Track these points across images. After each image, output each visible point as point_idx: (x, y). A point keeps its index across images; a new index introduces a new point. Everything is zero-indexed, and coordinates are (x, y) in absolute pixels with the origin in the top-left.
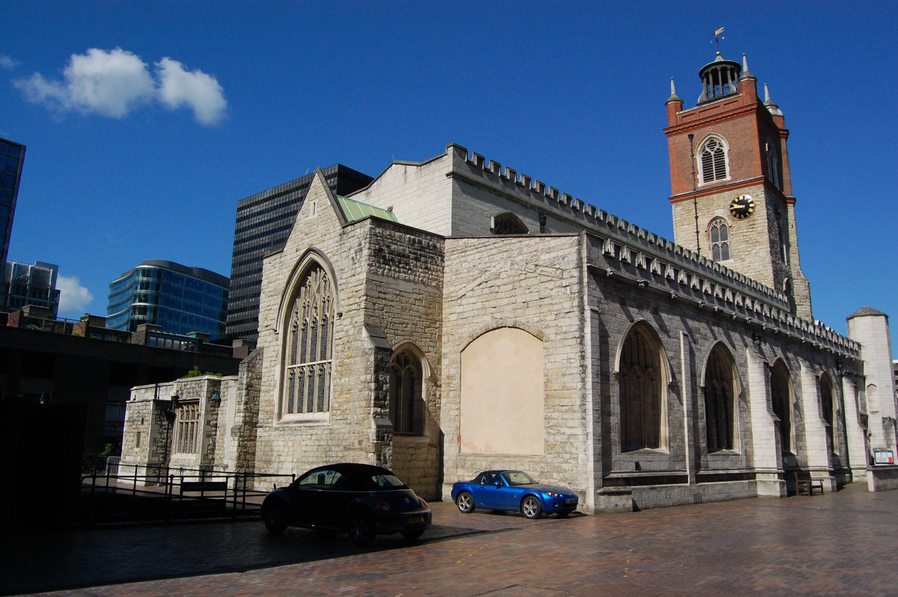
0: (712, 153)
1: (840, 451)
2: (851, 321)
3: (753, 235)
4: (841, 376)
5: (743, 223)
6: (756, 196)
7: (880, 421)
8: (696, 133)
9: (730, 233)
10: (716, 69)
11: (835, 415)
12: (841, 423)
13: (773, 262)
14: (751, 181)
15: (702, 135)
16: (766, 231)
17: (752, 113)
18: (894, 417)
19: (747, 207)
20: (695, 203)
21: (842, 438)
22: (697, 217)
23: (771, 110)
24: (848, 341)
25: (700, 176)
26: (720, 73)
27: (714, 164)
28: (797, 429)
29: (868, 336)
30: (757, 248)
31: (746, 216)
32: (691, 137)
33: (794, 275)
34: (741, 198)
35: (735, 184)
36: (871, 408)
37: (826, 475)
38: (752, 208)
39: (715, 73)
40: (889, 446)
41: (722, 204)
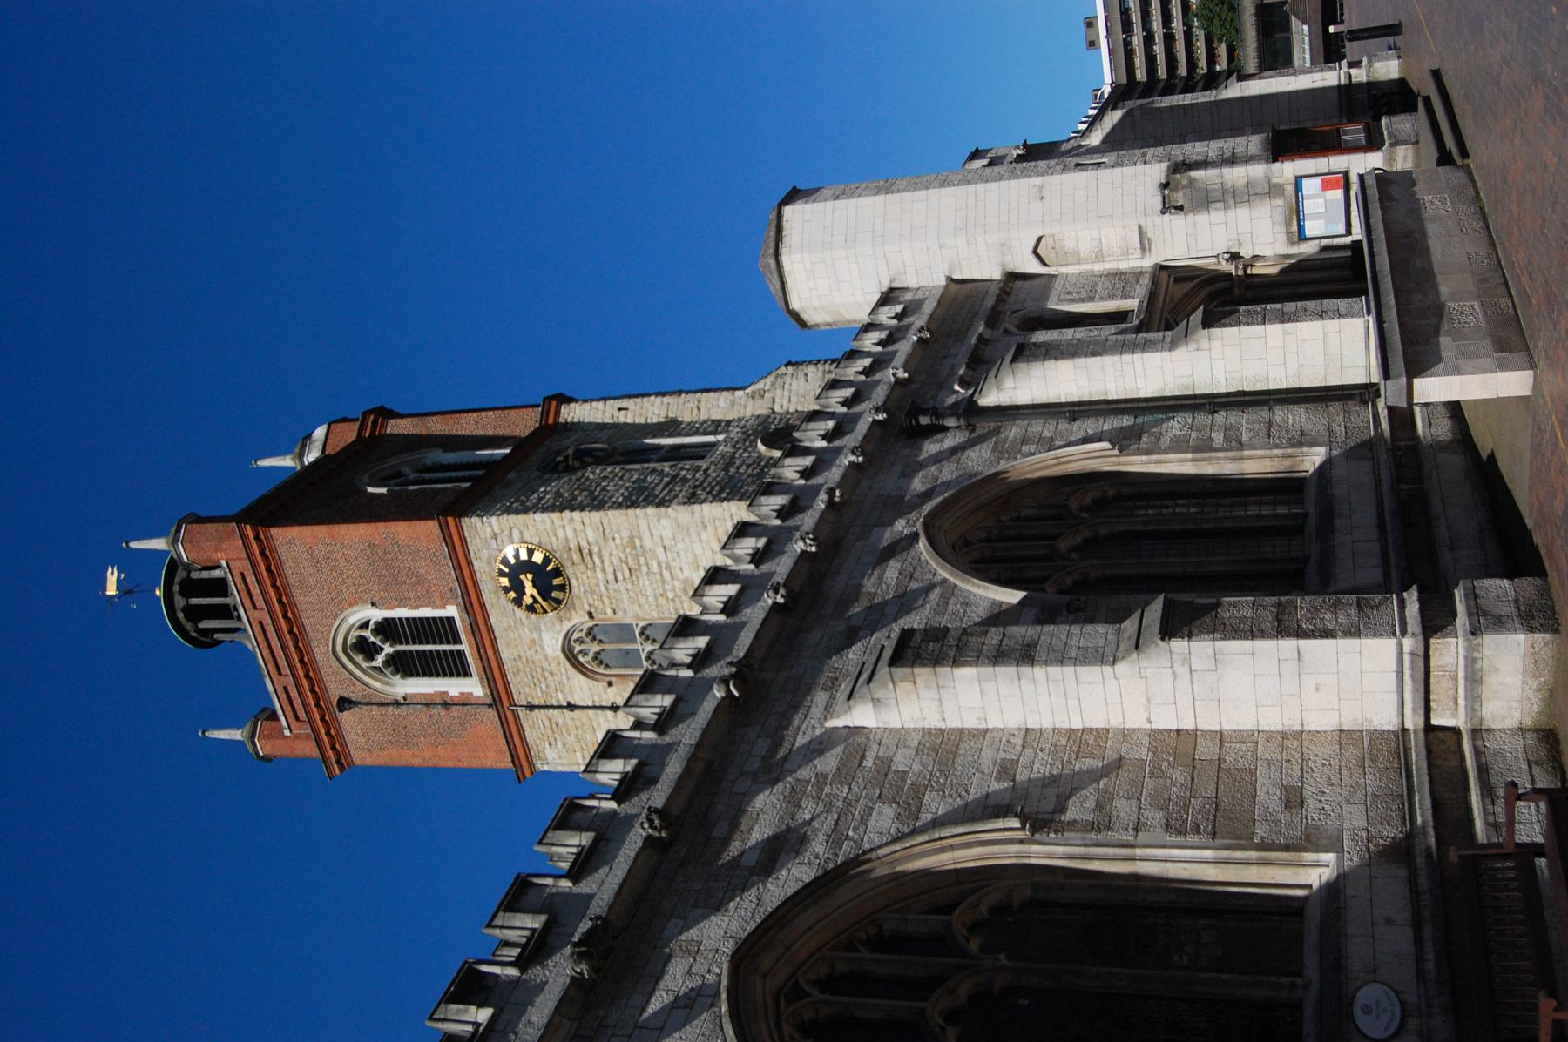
0: (388, 649)
1: (1302, 440)
2: (810, 317)
3: (613, 553)
4: (971, 411)
5: (579, 578)
6: (501, 538)
7: (1176, 221)
8: (335, 691)
9: (606, 616)
10: (184, 610)
11: (1137, 464)
12: (1176, 426)
13: (692, 499)
14: (453, 553)
15: (342, 675)
16: (596, 516)
17: (269, 538)
18: (1156, 171)
19: (528, 566)
20: (531, 707)
21: (1244, 421)
22: (571, 707)
23: (310, 458)
24: (853, 354)
25: (453, 687)
26: (195, 601)
27: (419, 647)
28: (1178, 828)
29: (850, 260)
30: (648, 544)
31: (557, 572)
32: (345, 703)
33: (761, 409)
34: (505, 581)
35: (466, 597)
36: (1126, 254)
37: (1449, 652)
38: (531, 552)
39: (195, 614)
40: (1274, 190)
41: (526, 634)
